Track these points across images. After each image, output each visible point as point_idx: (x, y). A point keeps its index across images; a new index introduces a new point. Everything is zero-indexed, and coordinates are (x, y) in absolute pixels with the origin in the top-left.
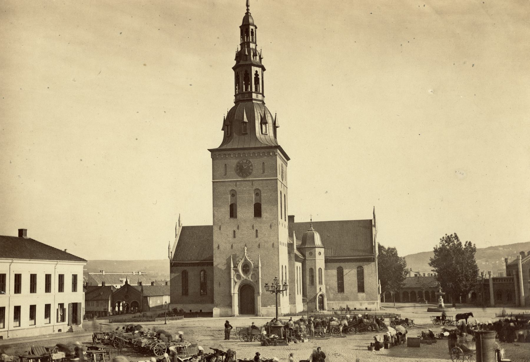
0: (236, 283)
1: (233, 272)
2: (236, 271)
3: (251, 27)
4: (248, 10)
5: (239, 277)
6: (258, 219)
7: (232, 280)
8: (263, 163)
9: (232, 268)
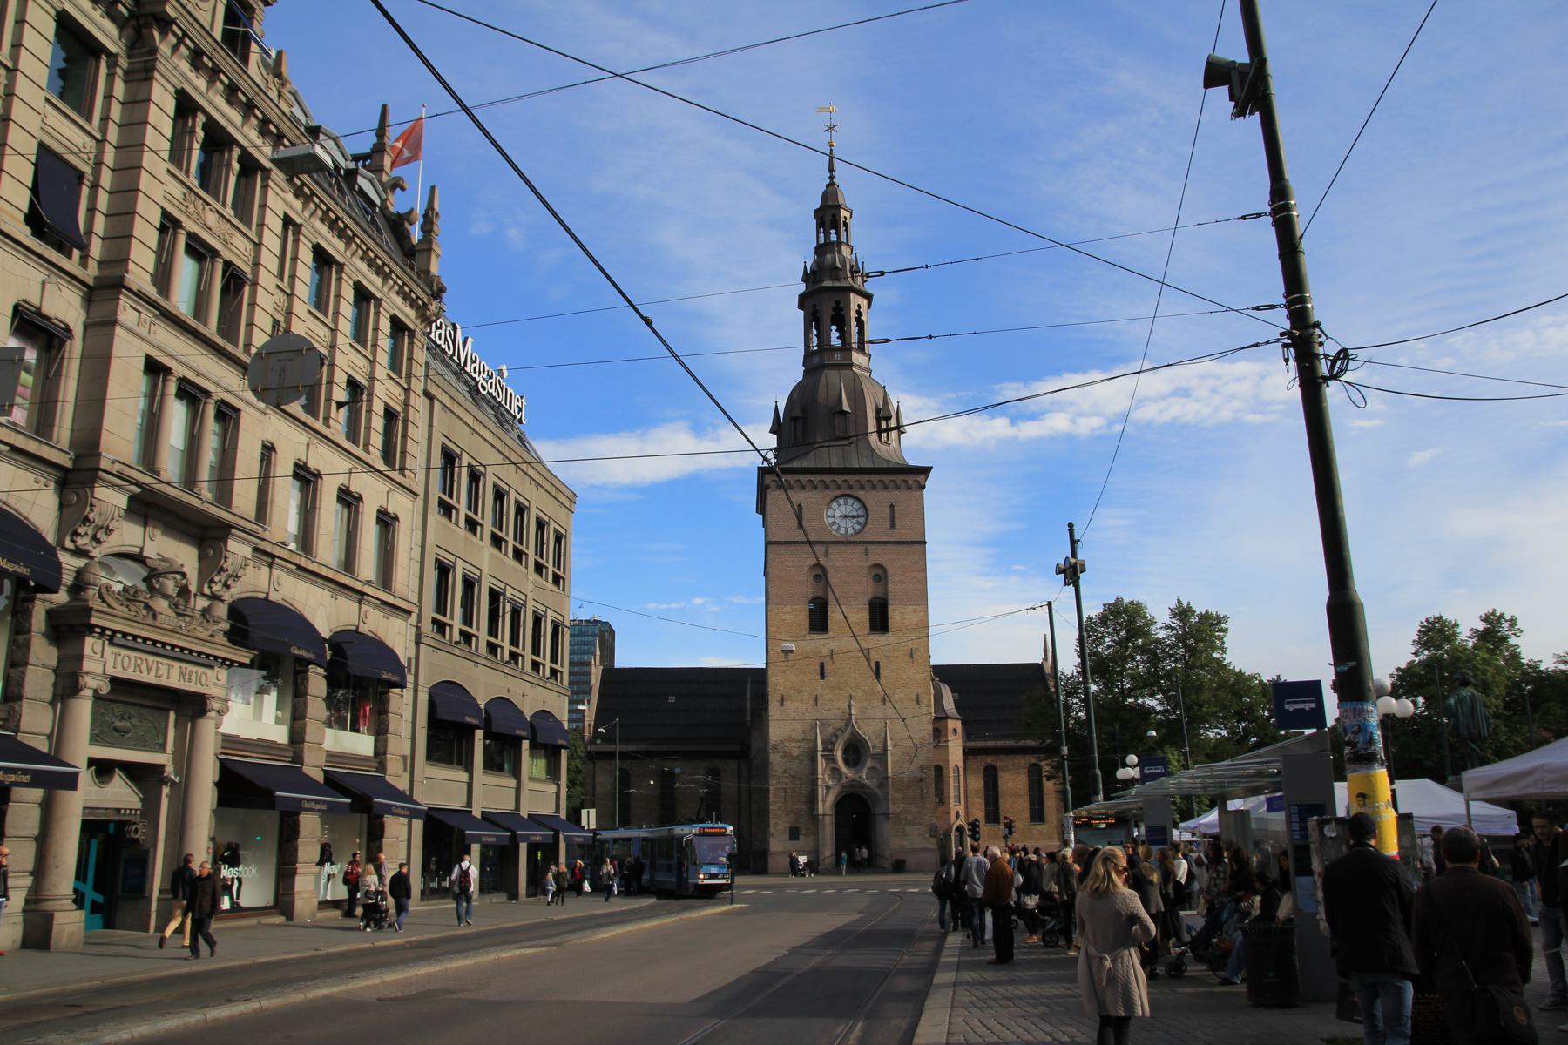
0: (828, 787)
1: (821, 763)
2: (830, 759)
3: (843, 213)
4: (831, 177)
5: (836, 772)
6: (879, 640)
7: (820, 782)
8: (892, 506)
9: (819, 753)
